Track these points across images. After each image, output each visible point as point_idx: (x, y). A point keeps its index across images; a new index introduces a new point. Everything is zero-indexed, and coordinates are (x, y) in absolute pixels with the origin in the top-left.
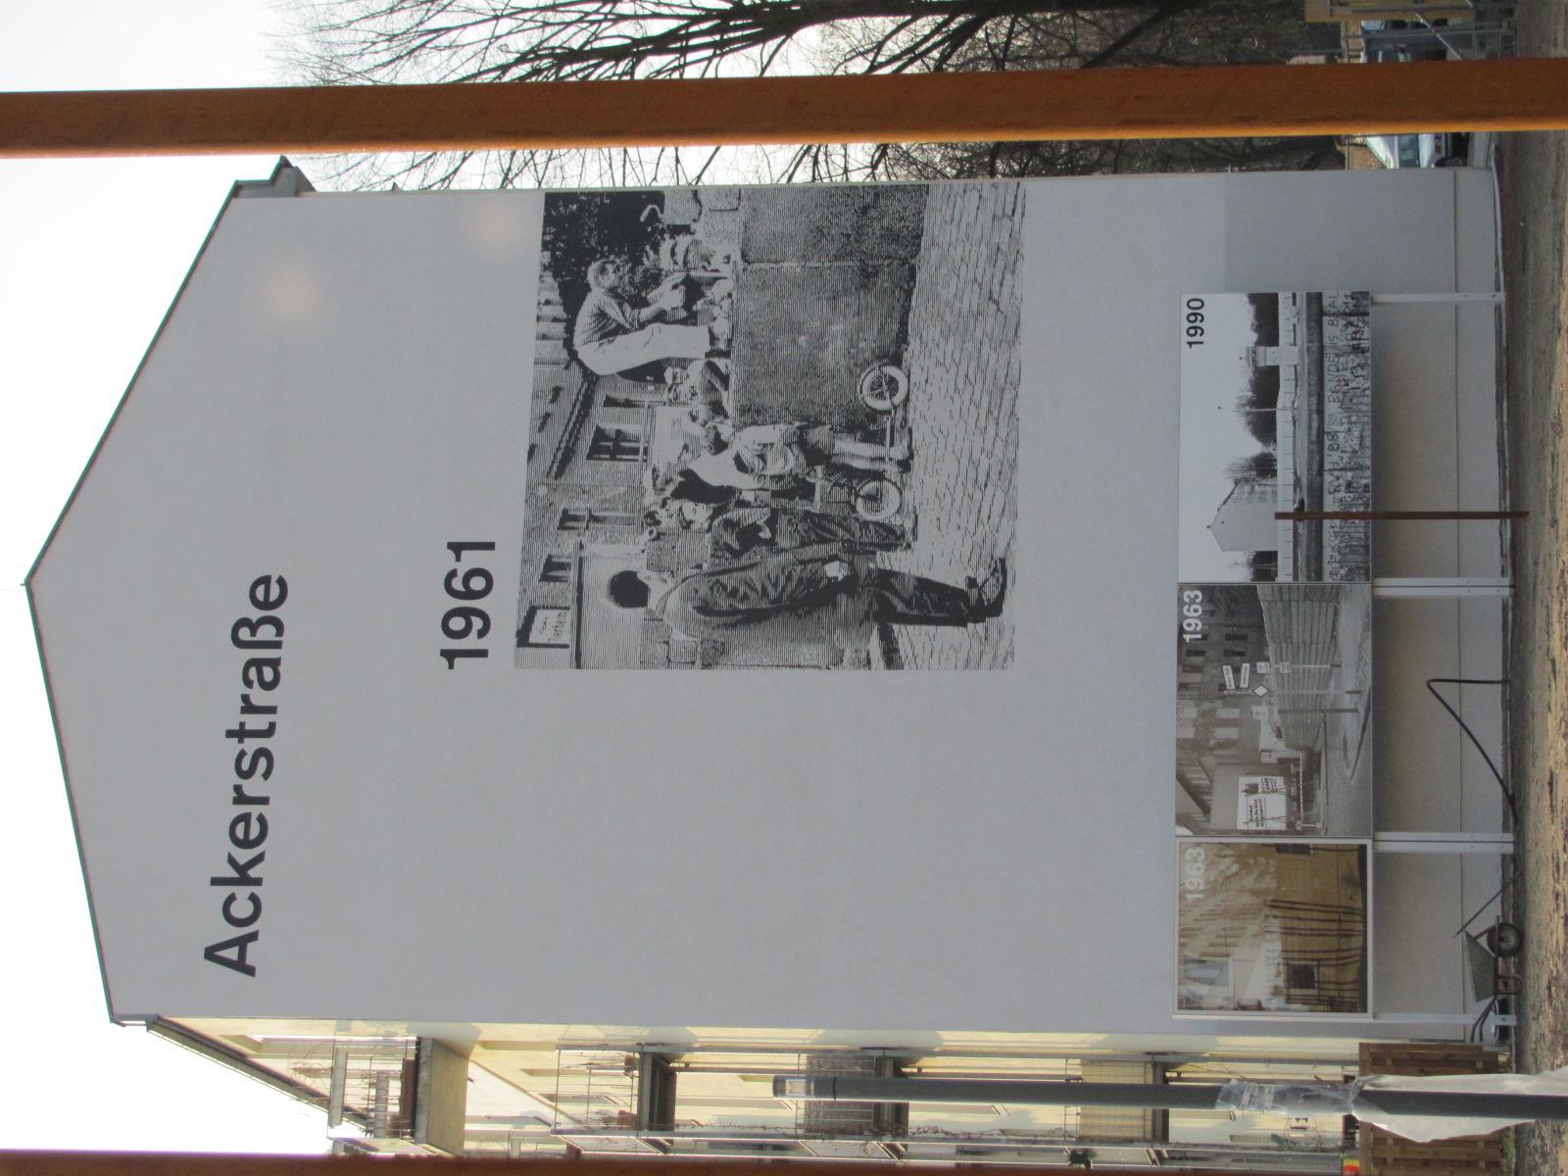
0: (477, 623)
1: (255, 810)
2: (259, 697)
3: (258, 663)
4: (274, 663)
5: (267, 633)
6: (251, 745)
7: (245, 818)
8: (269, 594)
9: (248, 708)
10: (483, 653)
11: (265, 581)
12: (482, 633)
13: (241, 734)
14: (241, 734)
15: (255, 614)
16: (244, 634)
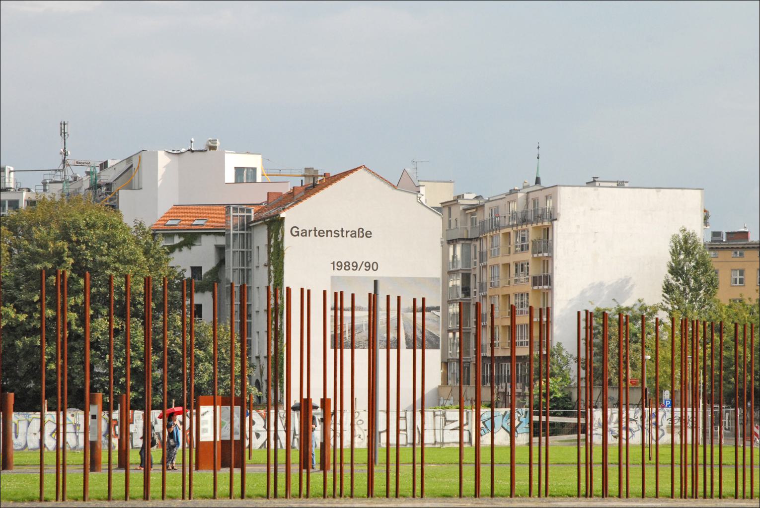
0: (339, 268)
1: (325, 234)
2: (349, 234)
3: (355, 234)
4: (355, 236)
5: (361, 234)
6: (340, 233)
7: (324, 233)
8: (368, 234)
9: (347, 232)
10: (334, 269)
11: (371, 234)
12: (338, 269)
13: (342, 231)
14: (342, 231)
15: (364, 232)
16: (361, 230)
